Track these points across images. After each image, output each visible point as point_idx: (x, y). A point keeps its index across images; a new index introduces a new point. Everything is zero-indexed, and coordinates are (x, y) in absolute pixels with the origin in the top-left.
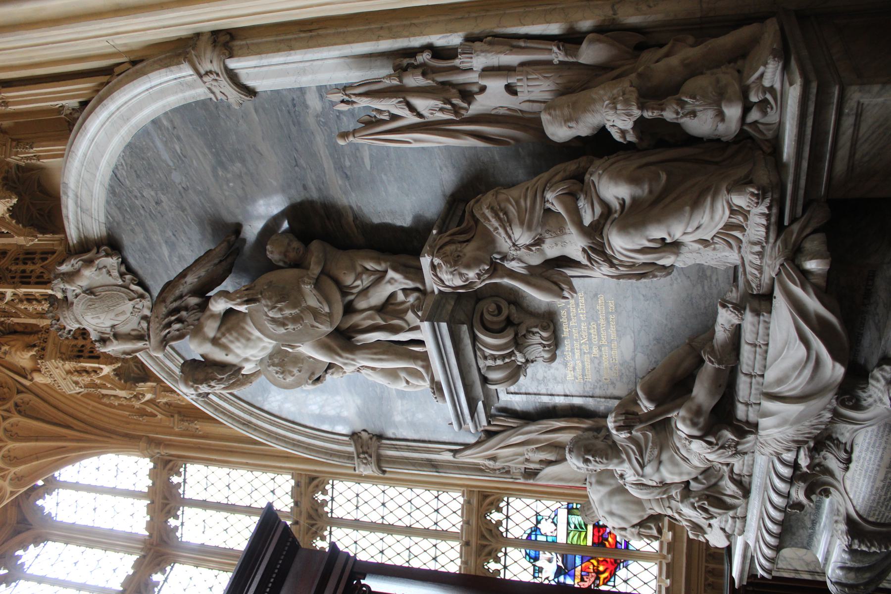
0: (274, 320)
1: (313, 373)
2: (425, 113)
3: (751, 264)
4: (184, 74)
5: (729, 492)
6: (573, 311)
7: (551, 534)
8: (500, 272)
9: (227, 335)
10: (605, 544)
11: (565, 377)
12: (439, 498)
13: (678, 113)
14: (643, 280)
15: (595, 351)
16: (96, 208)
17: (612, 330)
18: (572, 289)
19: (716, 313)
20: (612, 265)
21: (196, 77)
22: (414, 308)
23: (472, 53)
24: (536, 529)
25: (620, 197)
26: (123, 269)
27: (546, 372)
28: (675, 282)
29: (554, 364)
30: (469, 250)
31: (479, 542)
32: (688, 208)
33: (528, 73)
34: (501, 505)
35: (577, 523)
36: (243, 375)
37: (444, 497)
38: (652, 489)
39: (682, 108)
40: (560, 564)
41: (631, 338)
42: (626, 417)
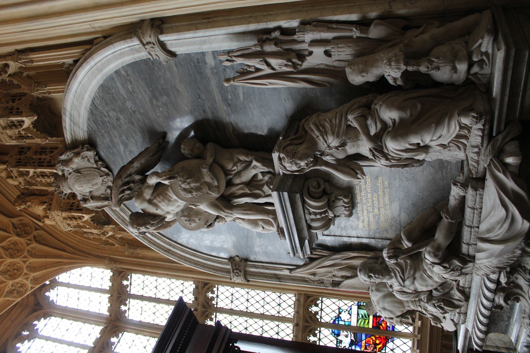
0: (185, 190)
1: (207, 222)
2: (276, 67)
3: (472, 159)
4: (134, 44)
5: (456, 298)
6: (363, 186)
7: (348, 321)
9: (157, 198)
10: (380, 327)
11: (358, 226)
12: (281, 297)
13: (428, 68)
14: (406, 169)
15: (376, 210)
16: (82, 122)
17: (387, 198)
18: (363, 173)
19: (450, 189)
20: (387, 159)
21: (141, 46)
22: (268, 184)
23: (304, 32)
24: (338, 317)
25: (393, 118)
26: (97, 158)
27: (346, 223)
28: (425, 170)
29: (351, 218)
30: (302, 149)
31: (304, 324)
32: (433, 125)
33: (338, 44)
34: (318, 302)
35: (363, 314)
36: (166, 222)
37: (284, 297)
38: (409, 295)
39: (431, 65)
40: (353, 338)
41: (398, 203)
42: (394, 250)
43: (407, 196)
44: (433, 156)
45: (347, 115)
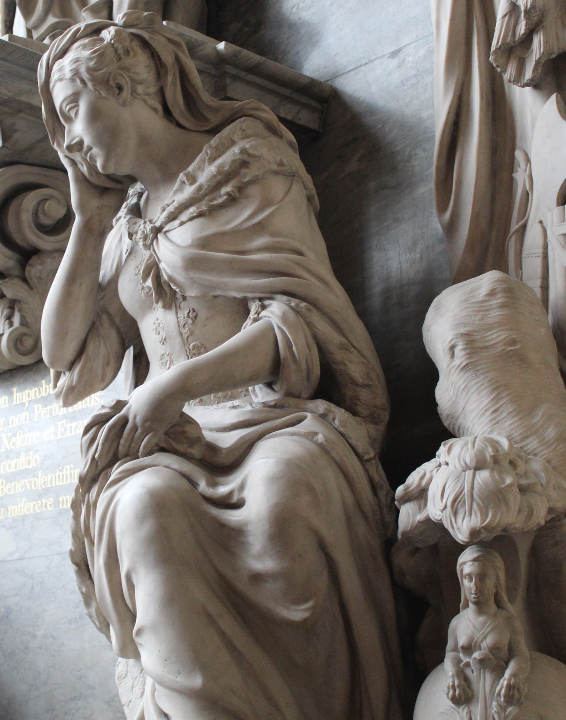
8: (95, 202)
13: (468, 649)
39: (482, 662)
43: (33, 587)
44: (130, 683)
45: (285, 298)
